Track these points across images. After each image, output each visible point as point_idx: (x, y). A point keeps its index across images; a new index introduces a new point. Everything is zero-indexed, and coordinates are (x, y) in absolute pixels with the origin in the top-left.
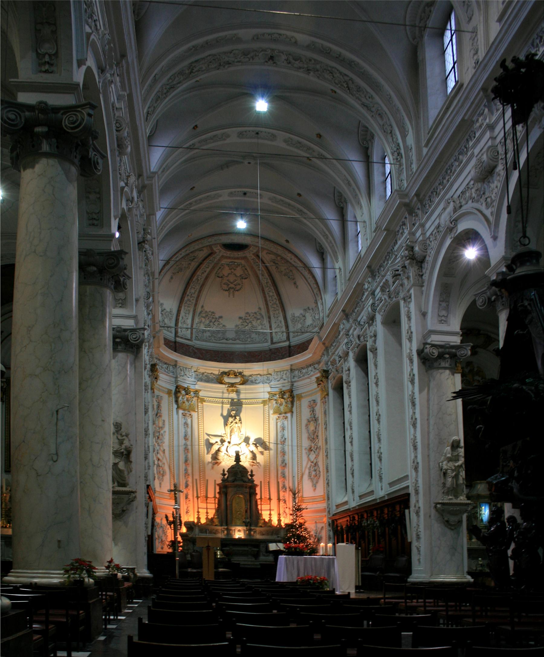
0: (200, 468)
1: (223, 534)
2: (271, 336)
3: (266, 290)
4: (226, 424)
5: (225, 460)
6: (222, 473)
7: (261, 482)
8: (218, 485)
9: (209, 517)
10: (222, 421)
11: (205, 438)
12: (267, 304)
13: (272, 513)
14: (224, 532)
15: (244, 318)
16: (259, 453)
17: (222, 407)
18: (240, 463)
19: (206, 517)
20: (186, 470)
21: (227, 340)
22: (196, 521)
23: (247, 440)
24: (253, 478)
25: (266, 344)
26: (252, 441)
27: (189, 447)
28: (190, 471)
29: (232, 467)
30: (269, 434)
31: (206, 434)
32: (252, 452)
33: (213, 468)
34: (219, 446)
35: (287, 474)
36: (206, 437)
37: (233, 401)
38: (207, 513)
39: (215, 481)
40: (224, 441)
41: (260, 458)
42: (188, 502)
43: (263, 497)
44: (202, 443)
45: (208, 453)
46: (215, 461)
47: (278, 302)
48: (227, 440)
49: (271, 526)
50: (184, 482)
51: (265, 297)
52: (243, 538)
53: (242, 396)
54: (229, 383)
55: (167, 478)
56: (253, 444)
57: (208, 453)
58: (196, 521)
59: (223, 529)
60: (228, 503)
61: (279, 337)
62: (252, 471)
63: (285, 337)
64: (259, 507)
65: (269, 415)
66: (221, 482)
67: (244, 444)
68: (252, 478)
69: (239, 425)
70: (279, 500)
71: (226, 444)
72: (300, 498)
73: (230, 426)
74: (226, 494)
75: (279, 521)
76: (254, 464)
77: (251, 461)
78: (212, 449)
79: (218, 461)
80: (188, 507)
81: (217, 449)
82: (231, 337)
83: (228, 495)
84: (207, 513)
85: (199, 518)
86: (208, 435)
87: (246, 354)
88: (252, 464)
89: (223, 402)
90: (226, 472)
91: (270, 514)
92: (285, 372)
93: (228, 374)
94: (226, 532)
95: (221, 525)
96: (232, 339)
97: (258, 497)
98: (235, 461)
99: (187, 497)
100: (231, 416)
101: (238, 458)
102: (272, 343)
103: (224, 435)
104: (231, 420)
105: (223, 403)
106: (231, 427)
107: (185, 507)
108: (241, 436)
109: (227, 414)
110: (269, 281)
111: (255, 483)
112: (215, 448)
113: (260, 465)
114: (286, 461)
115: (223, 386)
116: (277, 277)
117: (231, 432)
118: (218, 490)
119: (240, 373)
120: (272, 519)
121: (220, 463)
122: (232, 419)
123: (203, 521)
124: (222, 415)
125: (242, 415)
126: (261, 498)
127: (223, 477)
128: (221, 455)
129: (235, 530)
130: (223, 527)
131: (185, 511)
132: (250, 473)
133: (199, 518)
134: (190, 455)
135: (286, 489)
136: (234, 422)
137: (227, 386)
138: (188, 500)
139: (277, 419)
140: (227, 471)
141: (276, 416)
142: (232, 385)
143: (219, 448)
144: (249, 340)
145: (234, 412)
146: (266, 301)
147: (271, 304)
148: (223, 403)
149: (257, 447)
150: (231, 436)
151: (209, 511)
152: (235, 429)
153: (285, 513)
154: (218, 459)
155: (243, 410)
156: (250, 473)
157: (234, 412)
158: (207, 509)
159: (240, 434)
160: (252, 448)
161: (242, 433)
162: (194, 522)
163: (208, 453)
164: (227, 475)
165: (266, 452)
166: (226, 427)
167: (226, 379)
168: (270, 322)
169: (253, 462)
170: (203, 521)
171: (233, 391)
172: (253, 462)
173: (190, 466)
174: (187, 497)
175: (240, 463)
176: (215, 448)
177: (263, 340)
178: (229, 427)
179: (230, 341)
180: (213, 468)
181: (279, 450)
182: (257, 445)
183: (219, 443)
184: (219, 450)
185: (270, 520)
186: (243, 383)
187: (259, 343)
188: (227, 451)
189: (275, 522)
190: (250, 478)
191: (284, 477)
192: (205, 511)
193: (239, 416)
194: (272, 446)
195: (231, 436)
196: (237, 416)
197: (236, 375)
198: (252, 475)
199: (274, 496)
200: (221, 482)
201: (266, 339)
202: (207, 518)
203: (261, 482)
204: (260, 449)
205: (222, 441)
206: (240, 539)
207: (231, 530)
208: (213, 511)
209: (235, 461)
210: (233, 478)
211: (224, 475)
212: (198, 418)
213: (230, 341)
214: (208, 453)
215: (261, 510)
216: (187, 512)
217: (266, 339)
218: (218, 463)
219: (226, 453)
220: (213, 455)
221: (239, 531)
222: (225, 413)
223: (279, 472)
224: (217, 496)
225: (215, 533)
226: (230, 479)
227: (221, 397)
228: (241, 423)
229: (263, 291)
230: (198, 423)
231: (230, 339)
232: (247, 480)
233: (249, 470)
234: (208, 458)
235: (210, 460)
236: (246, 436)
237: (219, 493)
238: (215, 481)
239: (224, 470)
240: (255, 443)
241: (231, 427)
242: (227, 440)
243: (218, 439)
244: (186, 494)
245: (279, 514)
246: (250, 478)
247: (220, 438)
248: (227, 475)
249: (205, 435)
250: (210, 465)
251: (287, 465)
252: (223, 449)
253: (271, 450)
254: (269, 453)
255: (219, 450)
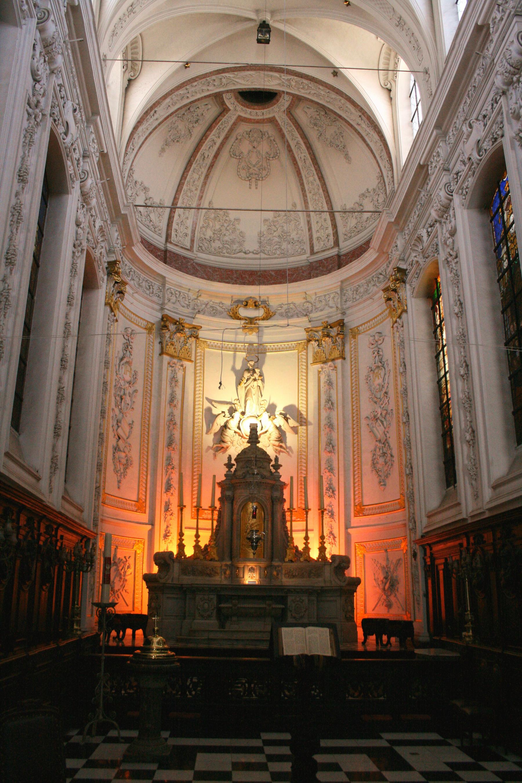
0: (193, 457)
1: (223, 577)
2: (310, 244)
3: (303, 173)
4: (238, 383)
5: (235, 443)
6: (227, 462)
7: (292, 478)
8: (219, 484)
9: (200, 544)
10: (232, 378)
11: (204, 407)
12: (305, 195)
13: (310, 534)
14: (225, 573)
15: (271, 219)
16: (290, 430)
17: (235, 357)
18: (258, 445)
19: (194, 543)
20: (169, 459)
21: (245, 253)
22: (175, 552)
23: (271, 409)
24: (279, 471)
25: (304, 257)
26: (279, 409)
27: (178, 420)
28: (176, 463)
29: (244, 452)
30: (307, 398)
31: (207, 399)
32: (279, 428)
33: (215, 456)
34: (225, 419)
35: (335, 465)
36: (207, 404)
37: (251, 347)
38: (197, 536)
39: (214, 476)
40: (235, 410)
41: (291, 439)
42: (169, 517)
43: (295, 506)
44: (200, 415)
45: (207, 432)
46: (219, 445)
47: (321, 191)
48: (240, 410)
49: (309, 560)
50: (165, 481)
51: (302, 184)
52: (257, 583)
53: (266, 338)
54: (245, 319)
55: (133, 471)
56: (281, 414)
57: (208, 432)
58: (175, 552)
59: (224, 567)
60: (235, 517)
61: (322, 243)
62: (277, 459)
63: (331, 243)
64: (288, 524)
65: (307, 367)
66: (224, 478)
67: (266, 415)
68: (277, 472)
69: (260, 383)
70: (322, 511)
71: (237, 415)
72: (358, 507)
73: (246, 385)
74: (232, 500)
75: (322, 549)
76: (282, 450)
77: (277, 443)
78: (215, 424)
79: (224, 445)
80: (167, 527)
81: (223, 424)
82: (251, 250)
83: (234, 503)
84: (197, 536)
85: (181, 546)
86: (210, 401)
87: (273, 273)
88: (279, 449)
89: (236, 349)
90: (233, 462)
91: (307, 538)
92: (332, 296)
93: (244, 303)
94: (228, 572)
95: (221, 559)
96: (253, 253)
97: (286, 506)
98: (248, 442)
99: (167, 509)
100: (248, 370)
101: (254, 437)
102: (312, 253)
103: (235, 402)
104: (247, 375)
105: (235, 350)
106: (246, 387)
107: (164, 527)
108: (262, 403)
109: (242, 367)
110: (308, 156)
111: (282, 479)
112: (220, 421)
113: (292, 452)
114: (335, 442)
115: (237, 322)
116: (318, 147)
117: (246, 396)
118: (218, 495)
119: (264, 302)
120: (310, 546)
121: (227, 447)
122: (249, 375)
123: (189, 552)
124: (233, 369)
125: (266, 369)
126: (291, 510)
127: (227, 470)
128: (230, 433)
129: (244, 568)
130: (224, 563)
131: (163, 533)
132: (273, 463)
133: (181, 546)
134: (177, 434)
135: (333, 492)
136: (252, 378)
137: (243, 322)
138: (168, 513)
139: (319, 372)
140: (235, 460)
141: (318, 366)
142: (251, 320)
143: (227, 422)
144: (278, 252)
145: (252, 363)
146: (303, 190)
147: (311, 195)
148: (235, 350)
149: (286, 419)
150: (246, 401)
151: (201, 533)
152: (254, 391)
153: (333, 535)
154: (224, 442)
155: (267, 361)
156: (273, 463)
157: (252, 363)
158: (197, 529)
159: (260, 399)
160: (280, 421)
161: (263, 398)
162: (171, 553)
163: (208, 432)
164: (234, 467)
165: (302, 429)
166: (239, 387)
167: (243, 312)
168: (309, 222)
169: (281, 447)
170: (189, 552)
171: (251, 329)
172: (281, 447)
173: (178, 452)
174: (167, 509)
175: (258, 445)
176: (220, 421)
177: (299, 250)
178: (244, 389)
179: (251, 255)
180: (215, 456)
181: (323, 422)
182: (288, 416)
183: (227, 414)
184: (225, 427)
185: (307, 549)
186: (268, 317)
187: (293, 255)
188: (239, 428)
189: (314, 554)
190: (273, 470)
191: (331, 470)
192: (194, 532)
193: (260, 368)
194: (312, 417)
195: (246, 401)
196: (257, 368)
197: (256, 306)
198: (277, 466)
199: (313, 504)
200: (224, 478)
201: (303, 249)
202: (197, 547)
203: (292, 478)
204: (292, 422)
205: (232, 411)
206: (251, 587)
207: (238, 568)
208: (209, 534)
209: (248, 442)
210: (244, 471)
211: (229, 465)
212: (195, 374)
213: (251, 255)
214: (207, 432)
215: (291, 531)
216: (166, 536)
217: (303, 249)
218: (224, 449)
219: (238, 430)
220: (215, 434)
221: (252, 570)
222: (238, 366)
223: (323, 462)
224: (217, 504)
225: (210, 575)
226: (239, 473)
227: (234, 340)
228: (263, 380)
229: (299, 173)
230: (195, 381)
231: (250, 252)
232: (267, 474)
233: (273, 457)
234: (209, 440)
235: (211, 444)
236: (271, 403)
237: (220, 499)
238: (214, 476)
239: (230, 458)
240: (283, 412)
241: (246, 387)
242: (240, 410)
243: (226, 408)
244: (166, 503)
245: (322, 537)
246: (273, 470)
247: (228, 406)
248: (234, 467)
249: (205, 400)
250: (211, 452)
251: (336, 448)
252: (233, 424)
253: (311, 424)
254: (307, 430)
255: (225, 427)
